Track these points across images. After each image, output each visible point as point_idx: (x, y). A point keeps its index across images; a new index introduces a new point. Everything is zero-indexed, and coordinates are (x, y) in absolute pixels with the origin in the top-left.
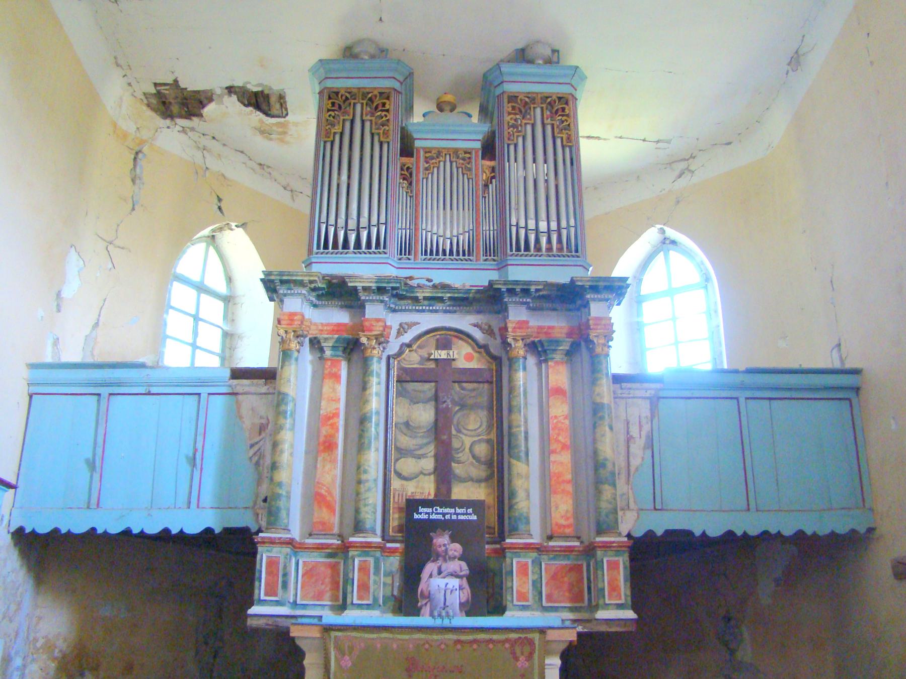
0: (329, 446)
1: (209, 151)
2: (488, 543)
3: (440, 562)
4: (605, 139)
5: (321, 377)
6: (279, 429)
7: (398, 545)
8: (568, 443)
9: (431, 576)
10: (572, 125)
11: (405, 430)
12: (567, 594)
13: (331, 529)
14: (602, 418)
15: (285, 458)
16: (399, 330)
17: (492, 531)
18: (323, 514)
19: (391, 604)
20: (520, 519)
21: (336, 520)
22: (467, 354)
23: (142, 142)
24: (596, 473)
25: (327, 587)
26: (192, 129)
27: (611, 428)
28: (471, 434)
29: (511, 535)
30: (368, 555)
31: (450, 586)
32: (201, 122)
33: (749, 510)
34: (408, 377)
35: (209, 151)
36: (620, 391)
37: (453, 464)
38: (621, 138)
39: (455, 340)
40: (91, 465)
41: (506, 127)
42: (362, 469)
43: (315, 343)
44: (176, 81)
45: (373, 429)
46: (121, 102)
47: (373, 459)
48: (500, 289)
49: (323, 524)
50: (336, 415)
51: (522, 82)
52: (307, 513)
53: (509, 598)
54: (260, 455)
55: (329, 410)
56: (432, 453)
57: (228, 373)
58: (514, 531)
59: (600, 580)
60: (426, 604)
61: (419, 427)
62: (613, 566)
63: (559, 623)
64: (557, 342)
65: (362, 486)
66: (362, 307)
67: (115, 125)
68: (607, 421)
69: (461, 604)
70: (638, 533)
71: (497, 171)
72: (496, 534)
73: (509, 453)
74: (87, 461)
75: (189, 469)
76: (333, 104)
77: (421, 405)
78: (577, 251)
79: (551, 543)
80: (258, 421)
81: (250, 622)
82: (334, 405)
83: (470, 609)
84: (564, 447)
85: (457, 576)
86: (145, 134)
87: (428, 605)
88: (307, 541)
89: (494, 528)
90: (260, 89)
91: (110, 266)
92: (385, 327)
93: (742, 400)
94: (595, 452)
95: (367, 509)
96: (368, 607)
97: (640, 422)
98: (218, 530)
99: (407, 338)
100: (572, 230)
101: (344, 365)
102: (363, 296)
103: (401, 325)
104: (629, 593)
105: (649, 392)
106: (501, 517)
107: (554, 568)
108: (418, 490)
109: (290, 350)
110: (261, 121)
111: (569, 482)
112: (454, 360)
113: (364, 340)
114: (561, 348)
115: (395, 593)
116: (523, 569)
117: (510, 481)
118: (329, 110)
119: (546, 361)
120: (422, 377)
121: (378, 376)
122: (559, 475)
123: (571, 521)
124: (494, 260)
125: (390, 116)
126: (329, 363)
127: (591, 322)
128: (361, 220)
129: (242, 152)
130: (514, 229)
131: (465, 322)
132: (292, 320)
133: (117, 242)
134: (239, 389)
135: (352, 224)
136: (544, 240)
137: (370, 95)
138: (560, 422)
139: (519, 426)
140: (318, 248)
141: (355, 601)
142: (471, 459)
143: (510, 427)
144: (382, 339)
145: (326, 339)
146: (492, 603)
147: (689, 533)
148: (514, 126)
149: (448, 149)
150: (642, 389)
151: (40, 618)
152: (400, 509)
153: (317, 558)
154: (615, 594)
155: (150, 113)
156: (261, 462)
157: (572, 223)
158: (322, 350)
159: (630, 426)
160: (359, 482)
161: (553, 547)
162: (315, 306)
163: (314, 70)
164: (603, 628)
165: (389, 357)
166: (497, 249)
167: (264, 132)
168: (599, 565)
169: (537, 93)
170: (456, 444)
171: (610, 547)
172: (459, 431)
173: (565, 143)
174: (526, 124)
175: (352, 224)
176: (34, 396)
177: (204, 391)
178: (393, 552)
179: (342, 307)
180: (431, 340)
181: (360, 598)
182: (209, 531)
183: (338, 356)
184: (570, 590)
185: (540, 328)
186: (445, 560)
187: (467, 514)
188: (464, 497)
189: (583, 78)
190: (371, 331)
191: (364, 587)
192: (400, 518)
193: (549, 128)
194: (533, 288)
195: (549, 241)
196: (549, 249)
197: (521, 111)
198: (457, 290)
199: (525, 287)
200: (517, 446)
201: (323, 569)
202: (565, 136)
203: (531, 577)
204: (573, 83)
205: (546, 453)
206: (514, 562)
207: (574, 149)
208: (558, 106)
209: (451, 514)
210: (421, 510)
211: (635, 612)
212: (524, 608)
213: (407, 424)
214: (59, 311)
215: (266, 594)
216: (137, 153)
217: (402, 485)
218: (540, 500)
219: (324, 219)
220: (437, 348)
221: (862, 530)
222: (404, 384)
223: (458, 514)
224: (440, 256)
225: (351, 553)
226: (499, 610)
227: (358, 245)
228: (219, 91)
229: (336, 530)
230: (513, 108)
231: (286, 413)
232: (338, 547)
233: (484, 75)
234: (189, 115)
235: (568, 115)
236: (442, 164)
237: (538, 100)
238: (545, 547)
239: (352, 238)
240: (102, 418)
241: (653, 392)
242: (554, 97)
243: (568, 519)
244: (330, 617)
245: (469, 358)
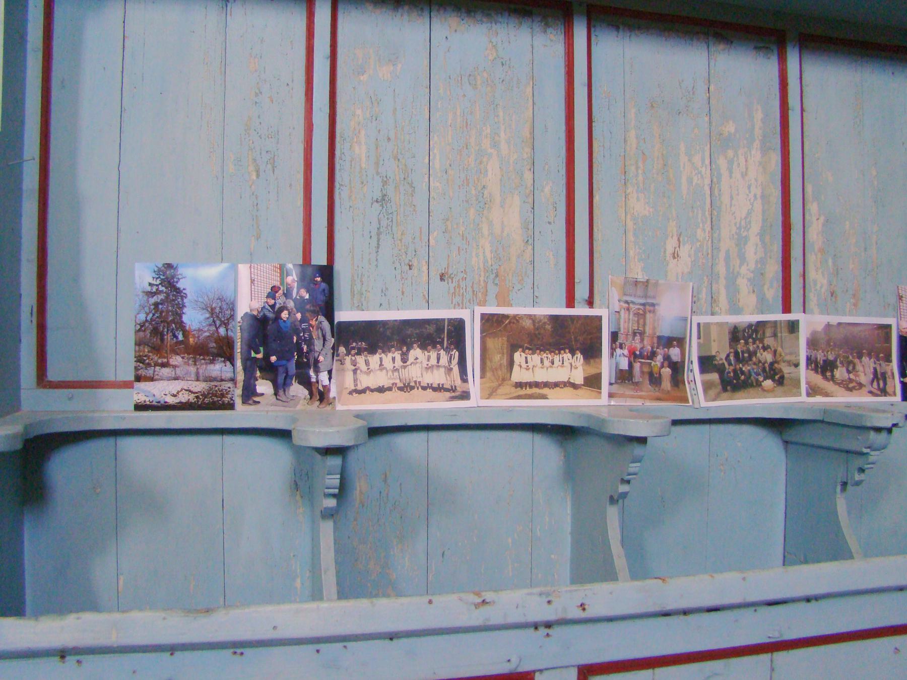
24: (654, 328)
28: (641, 321)
166: (646, 297)
218: (648, 330)
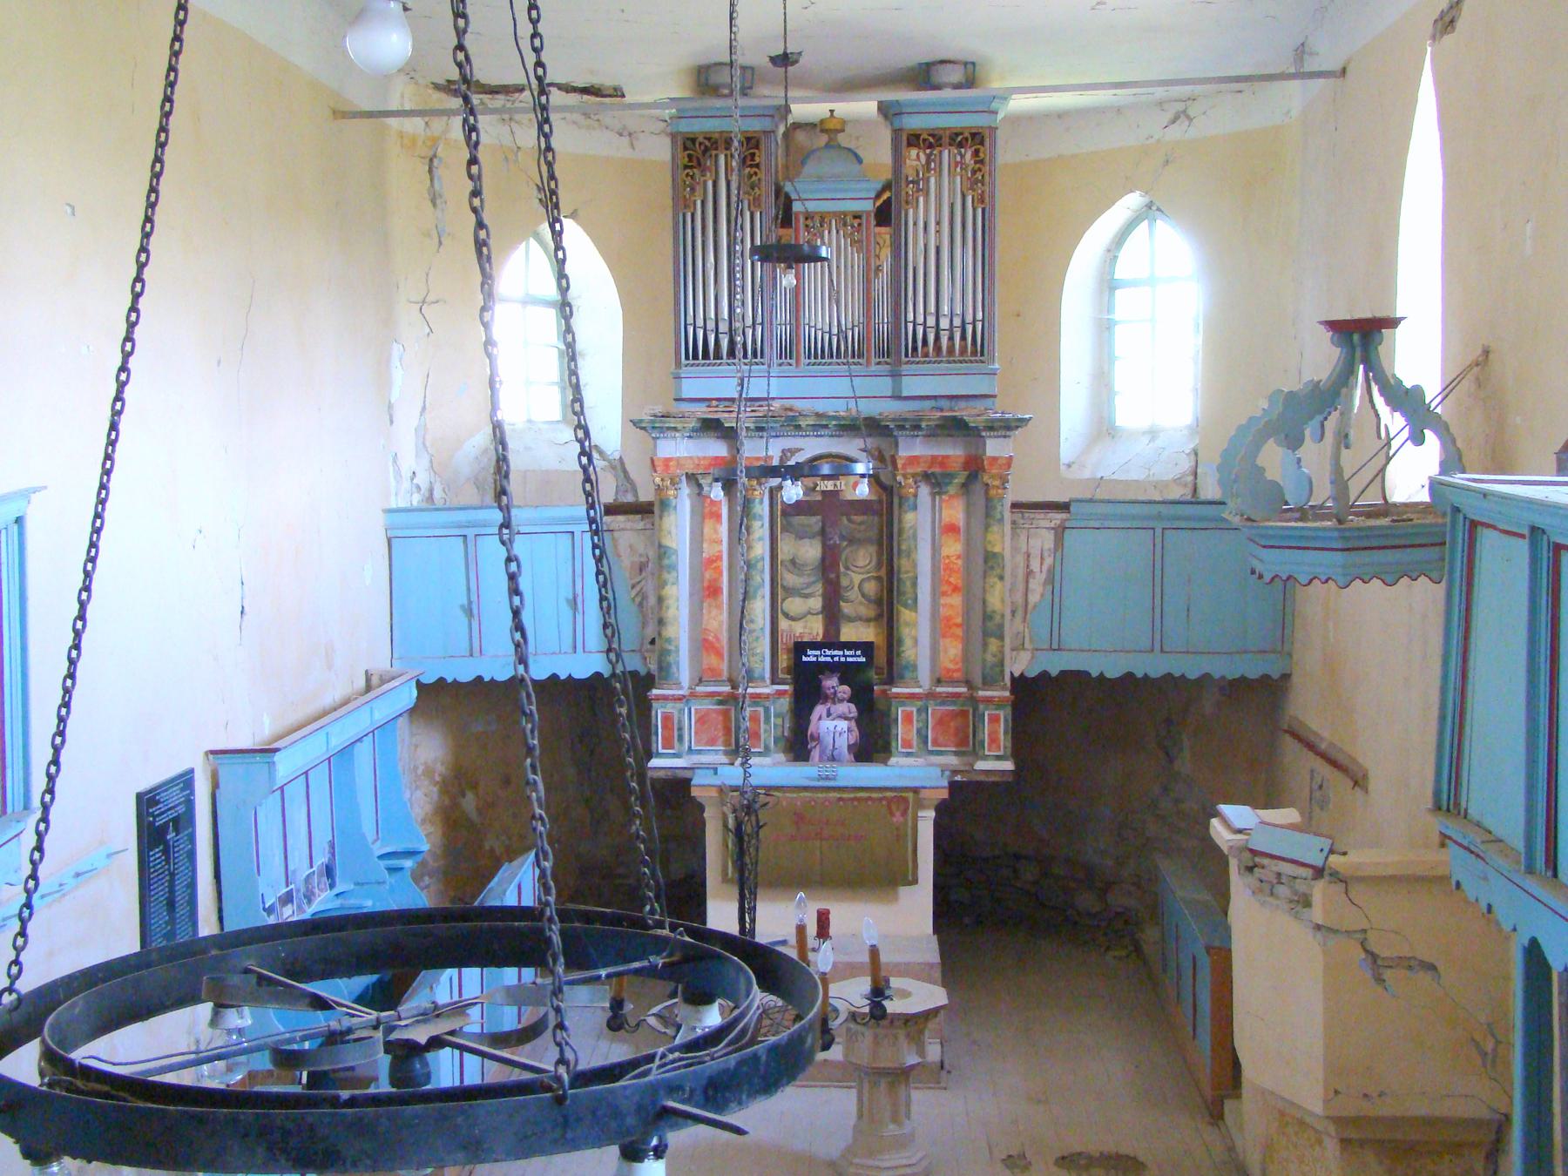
0: (713, 591)
5: (704, 512)
7: (786, 687)
13: (720, 675)
15: (670, 613)
18: (713, 660)
19: (782, 744)
40: (469, 611)
43: (692, 478)
47: (760, 608)
50: (719, 558)
52: (695, 657)
54: (644, 597)
62: (994, 719)
69: (850, 747)
70: (1032, 674)
74: (462, 607)
76: (690, 157)
79: (939, 690)
80: (636, 559)
82: (716, 548)
84: (956, 589)
85: (846, 719)
95: (757, 658)
104: (1009, 745)
106: (890, 662)
111: (958, 626)
116: (908, 718)
118: (686, 167)
119: (939, 493)
122: (948, 619)
125: (761, 175)
130: (910, 326)
140: (687, 358)
147: (1087, 674)
151: (416, 746)
153: (708, 705)
157: (979, 316)
164: (982, 778)
166: (893, 348)
168: (979, 718)
170: (844, 582)
172: (847, 568)
184: (956, 735)
185: (934, 458)
194: (923, 425)
195: (951, 338)
196: (951, 350)
205: (936, 594)
212: (908, 755)
213: (793, 562)
219: (690, 320)
221: (1275, 676)
229: (725, 675)
237: (946, 140)
242: (967, 134)
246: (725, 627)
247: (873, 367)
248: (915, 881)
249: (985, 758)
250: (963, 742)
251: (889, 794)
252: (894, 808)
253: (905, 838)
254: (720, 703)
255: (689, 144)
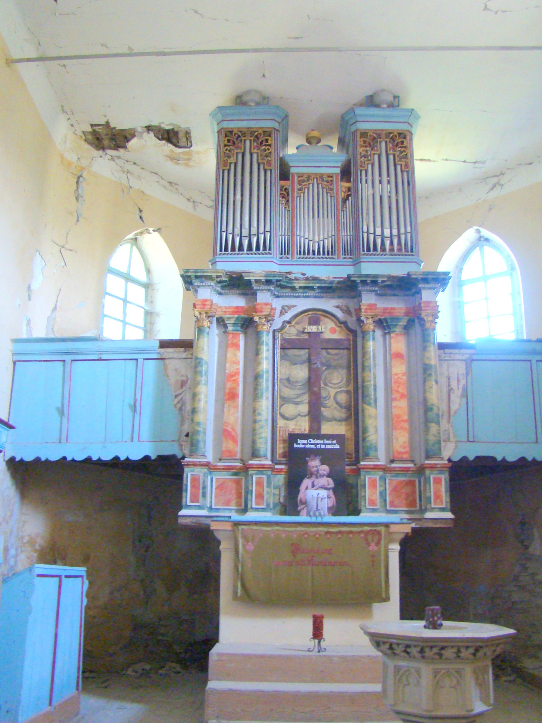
0: (232, 396)
1: (132, 174)
2: (348, 465)
3: (313, 478)
4: (434, 161)
6: (196, 384)
7: (283, 467)
8: (406, 393)
9: (307, 488)
10: (409, 155)
11: (287, 384)
12: (404, 502)
13: (235, 455)
14: (430, 375)
15: (202, 405)
16: (281, 311)
17: (350, 457)
18: (229, 445)
19: (279, 508)
20: (371, 448)
21: (238, 449)
22: (331, 328)
23: (82, 169)
24: (426, 414)
25: (233, 496)
26: (119, 157)
27: (437, 382)
29: (363, 460)
30: (263, 474)
31: (320, 496)
32: (126, 152)
33: (537, 442)
34: (288, 346)
35: (132, 174)
36: (443, 355)
37: (322, 409)
38: (446, 160)
39: (322, 318)
40: (61, 412)
41: (359, 156)
42: (257, 412)
43: (221, 322)
44: (108, 123)
45: (264, 384)
46: (66, 138)
47: (265, 405)
48: (354, 281)
49: (230, 452)
50: (237, 373)
51: (371, 122)
52: (217, 443)
53: (363, 504)
54: (182, 402)
55: (232, 370)
56: (307, 401)
57: (157, 344)
58: (366, 456)
59: (428, 491)
60: (303, 508)
61: (297, 382)
62: (438, 481)
63: (401, 522)
64: (398, 319)
65: (257, 424)
66: (255, 294)
67: (63, 158)
68: (433, 378)
71: (352, 190)
72: (353, 459)
73: (362, 399)
74: (58, 409)
75: (131, 414)
77: (298, 365)
78: (412, 251)
79: (393, 465)
81: (181, 521)
82: (236, 367)
83: (335, 511)
84: (403, 396)
85: (326, 489)
86: (84, 163)
87: (305, 508)
88: (219, 464)
89: (352, 455)
90: (171, 127)
91: (63, 264)
92: (272, 309)
93: (534, 362)
94: (425, 400)
95: (262, 440)
96: (263, 510)
97: (458, 378)
98: (153, 457)
99: (287, 317)
100: (409, 236)
101: (242, 337)
102: (255, 286)
103: (283, 307)
104: (448, 500)
105: (465, 355)
107: (395, 483)
108: (297, 427)
109: (203, 327)
110: (172, 151)
111: (405, 421)
112: (322, 332)
113: (256, 319)
114: (400, 324)
115: (282, 501)
116: (373, 484)
117: (363, 421)
118: (226, 146)
119: (389, 333)
120: (300, 345)
121: (267, 344)
122: (398, 417)
123: (407, 449)
124: (351, 258)
125: (272, 150)
126: (231, 336)
127: (422, 305)
128: (252, 229)
129: (156, 174)
130: (365, 235)
131: (329, 304)
132: (204, 305)
133: (67, 246)
134: (165, 356)
135: (245, 233)
136: (387, 243)
137: (256, 134)
138: (398, 378)
139: (370, 381)
140: (221, 250)
141: (254, 506)
142: (335, 405)
143: (363, 381)
144: (269, 318)
145: (229, 318)
146: (351, 507)
147: (493, 459)
148: (365, 156)
149: (316, 174)
150: (460, 354)
151: (24, 522)
152: (284, 441)
153: (226, 476)
154: (438, 501)
155: (87, 146)
156: (183, 407)
157: (409, 229)
158: (225, 326)
159: (451, 381)
160: (255, 422)
161: (394, 467)
162: (220, 294)
163: (213, 115)
164: (430, 525)
165: (274, 331)
166: (354, 249)
167: (174, 159)
168: (427, 480)
169: (382, 130)
170: (324, 394)
171: (435, 467)
172: (326, 384)
173: (403, 168)
174: (374, 154)
175: (245, 233)
176: (17, 363)
177: (140, 357)
178: (280, 472)
179: (240, 294)
180: (305, 318)
181: (257, 504)
182: (147, 458)
183: (237, 331)
184: (406, 499)
186: (317, 477)
187: (332, 444)
188: (330, 432)
189: (417, 117)
190: (262, 312)
191: (260, 496)
192: (284, 447)
193: (391, 157)
194: (380, 280)
195: (392, 243)
196: (392, 250)
197: (370, 144)
198: (324, 281)
199: (374, 279)
200: (368, 395)
201: (230, 484)
202: (403, 163)
203: (379, 489)
204: (410, 122)
206: (367, 478)
207: (410, 172)
208: (398, 140)
209: (320, 444)
210: (299, 441)
211: (453, 513)
212: (374, 510)
213: (288, 380)
214: (30, 299)
215: (192, 501)
216: (79, 177)
217: (286, 424)
218: (385, 434)
219: (224, 228)
220: (310, 324)
222: (285, 350)
223: (326, 444)
224: (311, 255)
225: (250, 472)
226: (356, 512)
227: (250, 248)
228: (140, 130)
229: (238, 456)
230: (365, 142)
231: (201, 372)
232: (241, 468)
233: (342, 117)
234: (117, 147)
235: (405, 147)
236: (311, 185)
238: (389, 468)
239: (246, 242)
240: (67, 378)
241: (468, 356)
243: (405, 448)
244: (236, 517)
245: (333, 331)
246: (240, 421)
247: (341, 259)
248: (387, 599)
249: (432, 510)
250: (412, 504)
251: (367, 528)
252: (370, 537)
253: (377, 563)
254: (235, 474)
255: (228, 134)
